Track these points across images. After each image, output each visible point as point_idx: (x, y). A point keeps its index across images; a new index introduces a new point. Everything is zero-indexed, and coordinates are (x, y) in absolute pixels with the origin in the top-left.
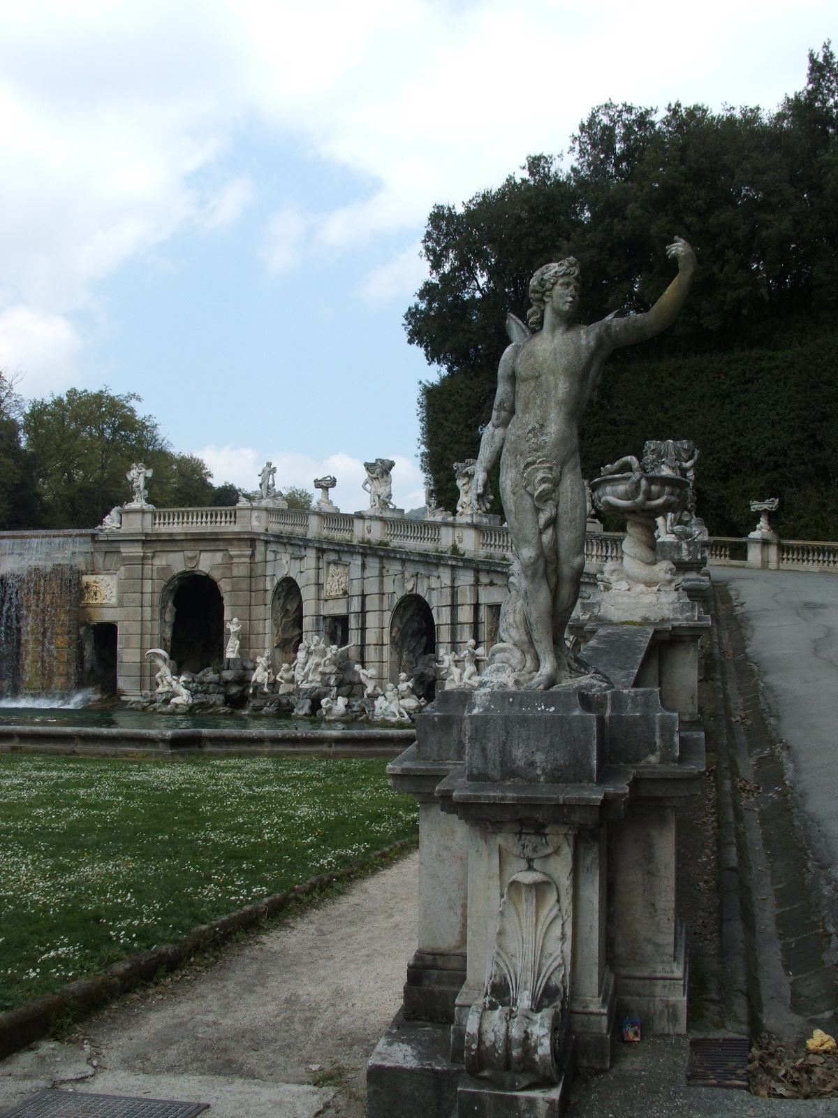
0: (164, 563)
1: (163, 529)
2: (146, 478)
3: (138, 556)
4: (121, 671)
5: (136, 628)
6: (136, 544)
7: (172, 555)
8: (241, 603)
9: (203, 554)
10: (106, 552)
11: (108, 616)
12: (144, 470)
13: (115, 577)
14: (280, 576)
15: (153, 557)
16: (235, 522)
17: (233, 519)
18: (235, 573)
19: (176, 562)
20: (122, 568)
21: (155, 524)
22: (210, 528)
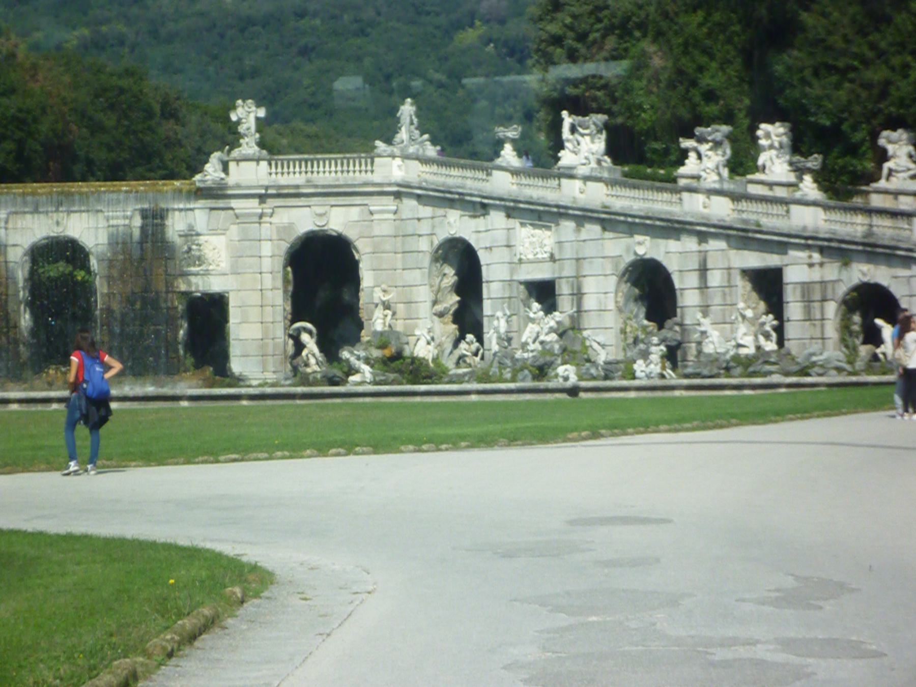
0: (285, 220)
1: (283, 180)
2: (258, 119)
3: (254, 214)
4: (235, 350)
5: (255, 298)
6: (251, 200)
7: (295, 210)
8: (384, 267)
9: (334, 209)
10: (212, 209)
11: (215, 285)
12: (254, 108)
13: (223, 238)
14: (443, 235)
15: (271, 215)
16: (372, 171)
17: (369, 168)
18: (377, 231)
19: (303, 220)
20: (234, 229)
21: (270, 174)
22: (342, 178)
